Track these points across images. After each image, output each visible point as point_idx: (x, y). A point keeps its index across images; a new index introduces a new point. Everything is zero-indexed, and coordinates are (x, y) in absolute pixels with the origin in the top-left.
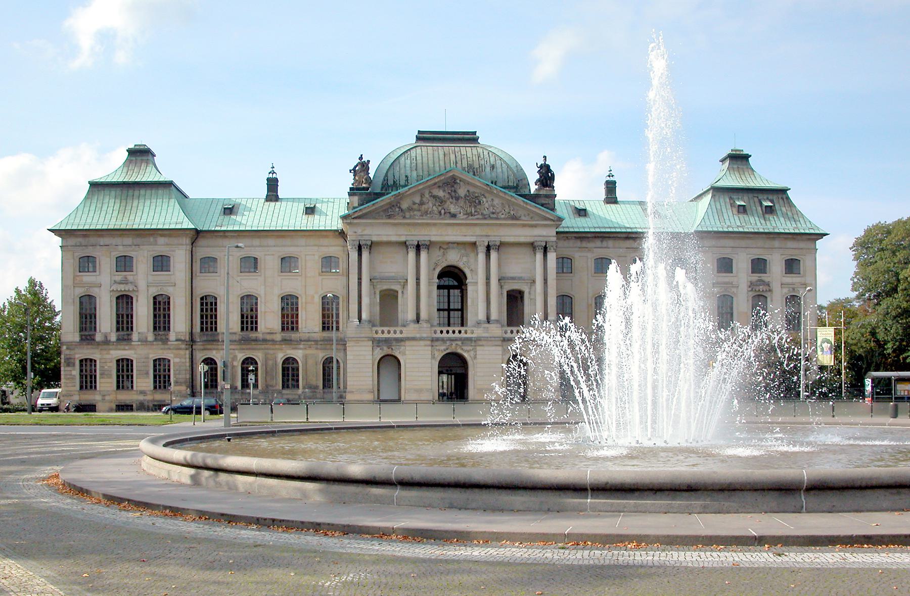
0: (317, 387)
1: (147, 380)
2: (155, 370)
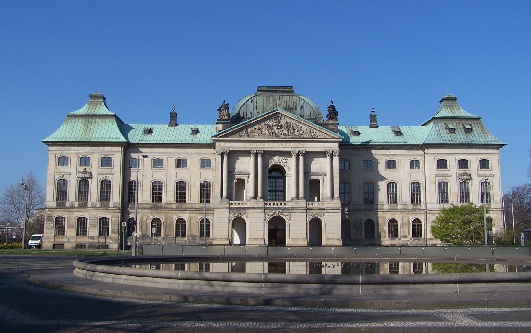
0: (196, 236)
2: (100, 225)
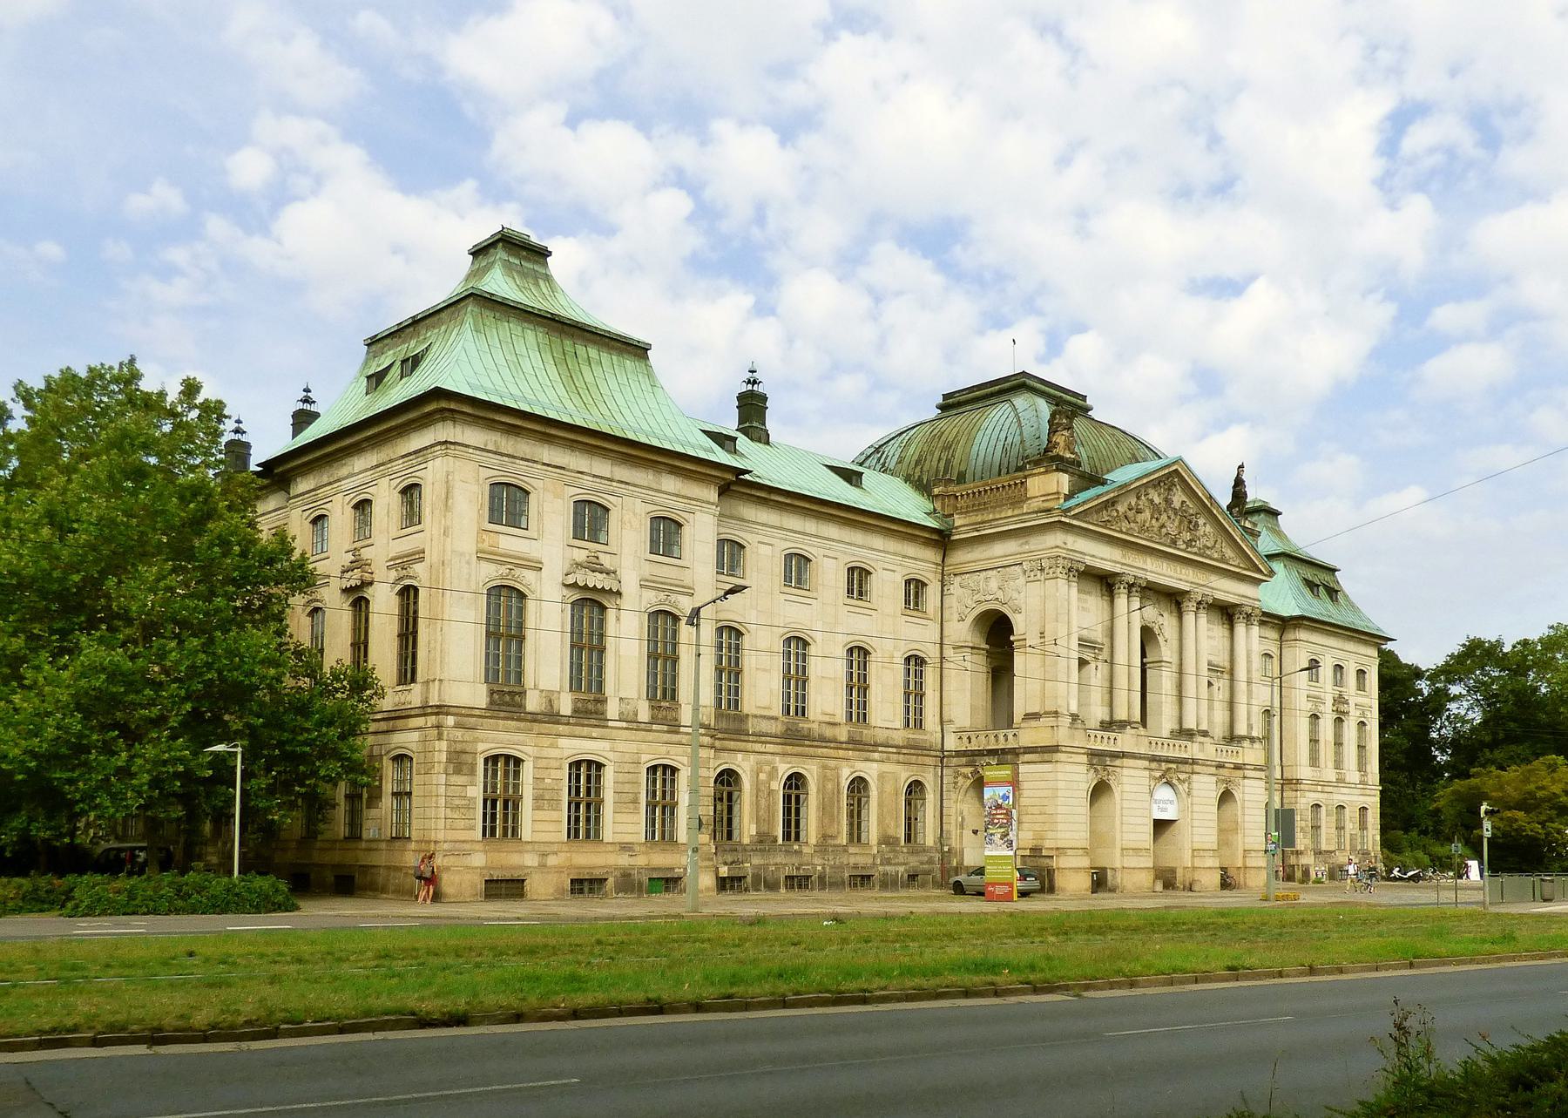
1: (634, 818)
